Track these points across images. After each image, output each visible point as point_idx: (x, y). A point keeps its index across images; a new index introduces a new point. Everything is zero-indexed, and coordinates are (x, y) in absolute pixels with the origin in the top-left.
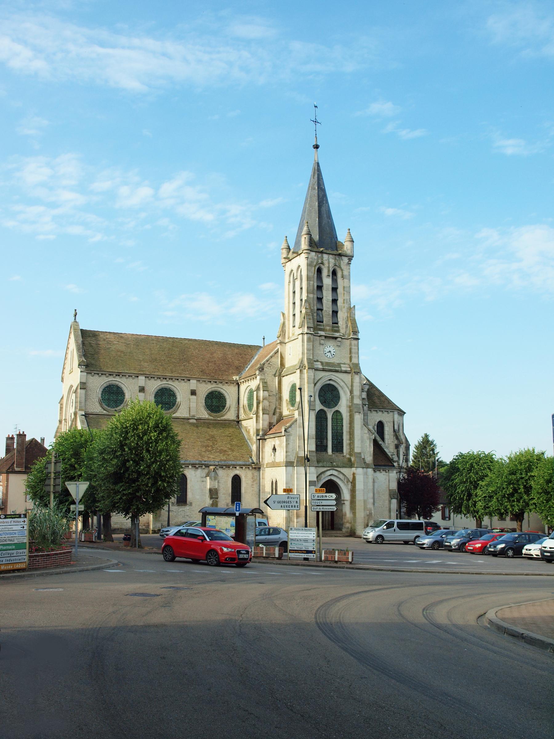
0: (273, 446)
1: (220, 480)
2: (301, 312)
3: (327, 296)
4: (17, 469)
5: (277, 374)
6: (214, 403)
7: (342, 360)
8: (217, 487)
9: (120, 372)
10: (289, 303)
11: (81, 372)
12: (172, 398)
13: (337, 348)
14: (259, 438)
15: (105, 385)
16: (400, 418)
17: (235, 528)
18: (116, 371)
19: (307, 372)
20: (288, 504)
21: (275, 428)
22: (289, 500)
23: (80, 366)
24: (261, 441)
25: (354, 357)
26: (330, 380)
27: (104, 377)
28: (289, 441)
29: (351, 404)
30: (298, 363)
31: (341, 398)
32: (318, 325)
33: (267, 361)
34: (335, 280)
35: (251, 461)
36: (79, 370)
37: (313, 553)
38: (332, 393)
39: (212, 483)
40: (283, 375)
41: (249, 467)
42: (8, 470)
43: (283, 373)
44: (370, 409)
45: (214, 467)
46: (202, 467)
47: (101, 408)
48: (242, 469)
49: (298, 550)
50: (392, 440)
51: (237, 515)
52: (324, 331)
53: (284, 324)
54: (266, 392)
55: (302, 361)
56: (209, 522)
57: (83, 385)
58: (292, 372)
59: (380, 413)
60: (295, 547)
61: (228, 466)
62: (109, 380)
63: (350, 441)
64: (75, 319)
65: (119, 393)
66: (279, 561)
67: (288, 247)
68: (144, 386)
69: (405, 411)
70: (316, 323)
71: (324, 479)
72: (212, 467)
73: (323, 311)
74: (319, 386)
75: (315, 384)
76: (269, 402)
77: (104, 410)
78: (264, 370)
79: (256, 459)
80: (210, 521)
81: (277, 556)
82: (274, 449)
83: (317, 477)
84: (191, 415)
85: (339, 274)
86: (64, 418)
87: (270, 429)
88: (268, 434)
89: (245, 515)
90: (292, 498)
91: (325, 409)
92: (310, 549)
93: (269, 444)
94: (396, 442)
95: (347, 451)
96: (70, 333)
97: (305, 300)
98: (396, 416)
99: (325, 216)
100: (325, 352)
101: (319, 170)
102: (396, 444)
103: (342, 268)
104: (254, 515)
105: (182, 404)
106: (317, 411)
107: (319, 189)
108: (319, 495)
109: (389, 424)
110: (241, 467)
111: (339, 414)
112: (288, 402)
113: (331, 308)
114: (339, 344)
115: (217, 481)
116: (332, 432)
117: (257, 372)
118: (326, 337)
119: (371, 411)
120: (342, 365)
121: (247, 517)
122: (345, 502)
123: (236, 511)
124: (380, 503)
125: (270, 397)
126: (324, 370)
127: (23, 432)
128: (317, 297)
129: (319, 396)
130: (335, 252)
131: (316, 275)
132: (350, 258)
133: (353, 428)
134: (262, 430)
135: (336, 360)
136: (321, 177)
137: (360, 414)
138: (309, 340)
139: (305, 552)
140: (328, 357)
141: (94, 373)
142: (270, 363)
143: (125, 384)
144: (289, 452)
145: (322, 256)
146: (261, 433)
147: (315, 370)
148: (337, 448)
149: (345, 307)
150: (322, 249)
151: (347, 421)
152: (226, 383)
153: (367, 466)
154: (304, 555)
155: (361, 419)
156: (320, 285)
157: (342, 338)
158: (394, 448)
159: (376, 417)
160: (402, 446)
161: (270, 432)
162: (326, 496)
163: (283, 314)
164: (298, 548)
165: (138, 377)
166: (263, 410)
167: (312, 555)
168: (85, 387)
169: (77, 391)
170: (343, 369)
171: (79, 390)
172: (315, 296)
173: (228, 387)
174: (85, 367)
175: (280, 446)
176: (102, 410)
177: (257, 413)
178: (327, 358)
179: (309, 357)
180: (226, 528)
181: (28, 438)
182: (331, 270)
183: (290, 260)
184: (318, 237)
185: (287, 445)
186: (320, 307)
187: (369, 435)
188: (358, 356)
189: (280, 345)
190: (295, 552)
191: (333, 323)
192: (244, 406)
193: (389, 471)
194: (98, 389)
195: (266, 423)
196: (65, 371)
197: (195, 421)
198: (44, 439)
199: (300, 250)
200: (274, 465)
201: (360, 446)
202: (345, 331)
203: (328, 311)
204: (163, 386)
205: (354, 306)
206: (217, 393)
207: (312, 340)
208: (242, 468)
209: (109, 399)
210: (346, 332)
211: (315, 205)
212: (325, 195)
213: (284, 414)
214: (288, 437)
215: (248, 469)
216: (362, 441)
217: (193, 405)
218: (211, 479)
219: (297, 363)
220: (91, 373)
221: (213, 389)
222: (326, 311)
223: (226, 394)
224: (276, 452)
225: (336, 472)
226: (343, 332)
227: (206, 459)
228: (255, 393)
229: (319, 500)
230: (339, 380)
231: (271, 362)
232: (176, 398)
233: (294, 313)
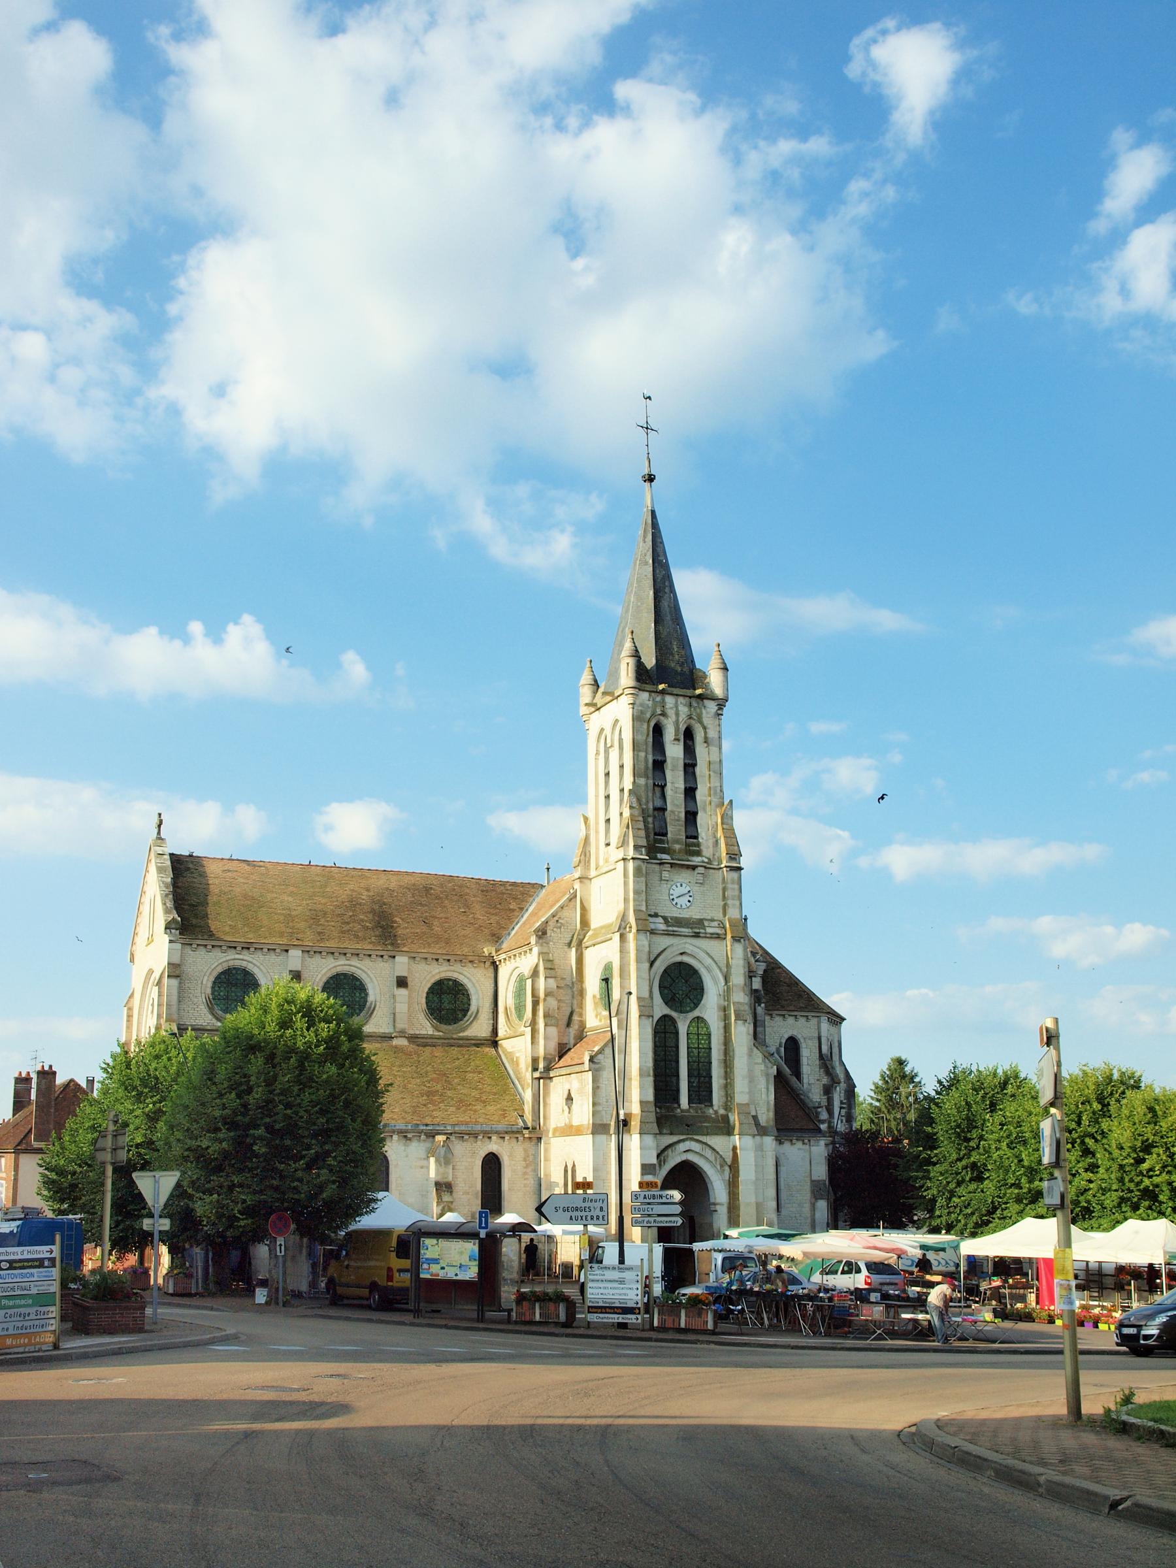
0: (566, 1093)
2: (621, 814)
3: (675, 781)
4: (36, 1145)
5: (574, 943)
6: (445, 1004)
8: (450, 1179)
9: (251, 941)
10: (597, 796)
11: (171, 941)
12: (358, 995)
13: (696, 888)
14: (537, 1075)
15: (220, 969)
16: (833, 1029)
17: (477, 1263)
18: (242, 940)
19: (637, 940)
20: (584, 1214)
21: (570, 1054)
22: (587, 1204)
23: (168, 930)
24: (541, 1081)
26: (681, 954)
27: (217, 953)
28: (598, 1081)
29: (726, 1003)
30: (617, 918)
31: (705, 990)
32: (656, 841)
33: (554, 916)
34: (689, 750)
35: (521, 1124)
36: (166, 938)
37: (635, 1313)
38: (686, 982)
39: (442, 1170)
40: (587, 944)
41: (517, 1136)
42: (17, 1146)
43: (587, 941)
44: (769, 1011)
45: (444, 1137)
47: (210, 1017)
48: (502, 1141)
49: (605, 1308)
50: (817, 1077)
51: (481, 1236)
52: (668, 854)
53: (587, 840)
54: (551, 981)
55: (624, 915)
56: (426, 1251)
57: (175, 970)
58: (602, 938)
59: (791, 1020)
60: (600, 1301)
61: (474, 1135)
62: (228, 958)
63: (727, 1080)
64: (159, 833)
65: (248, 984)
66: (569, 1331)
67: (593, 683)
68: (300, 969)
69: (843, 1015)
70: (652, 836)
71: (674, 1160)
72: (440, 1138)
73: (667, 813)
74: (660, 966)
75: (652, 964)
76: (559, 1001)
79: (533, 1120)
80: (427, 1249)
81: (563, 1317)
82: (569, 1098)
83: (658, 1156)
84: (397, 1030)
85: (699, 736)
86: (134, 1037)
87: (560, 1057)
88: (556, 1066)
89: (498, 1235)
90: (591, 1201)
91: (674, 1014)
92: (631, 1304)
93: (558, 1087)
94: (825, 1080)
95: (719, 1101)
96: (149, 861)
97: (630, 790)
98: (825, 1026)
99: (668, 618)
101: (655, 525)
102: (824, 1085)
103: (705, 725)
104: (518, 1235)
105: (377, 1007)
106: (656, 1019)
107: (656, 565)
108: (647, 1193)
109: (810, 1043)
111: (703, 1025)
112: (597, 1000)
114: (700, 878)
115: (451, 1167)
116: (688, 1062)
117: (533, 940)
118: (672, 865)
119: (771, 1015)
120: (706, 923)
121: (502, 1241)
122: (718, 1207)
123: (480, 1227)
124: (791, 1209)
125: (561, 991)
126: (667, 934)
127: (51, 1067)
128: (654, 784)
129: (659, 987)
130: (689, 692)
131: (650, 739)
132: (722, 703)
133: (731, 1054)
134: (544, 1058)
136: (659, 540)
137: (747, 1024)
138: (638, 872)
139: (620, 1311)
140: (679, 906)
141: (198, 945)
142: (560, 921)
143: (261, 967)
144: (599, 1104)
145: (663, 700)
146: (541, 1066)
147: (651, 933)
149: (713, 804)
150: (661, 687)
151: (718, 1039)
152: (470, 962)
153: (762, 1131)
154: (618, 1318)
155: (749, 1034)
156: (660, 758)
157: (705, 867)
158: (822, 1093)
159: (780, 1028)
160: (838, 1089)
161: (562, 1063)
162: (661, 1197)
163: (586, 819)
164: (606, 1303)
165: (287, 951)
166: (545, 1017)
167: (634, 1316)
168: (177, 973)
169: (163, 981)
170: (709, 930)
171: (166, 980)
172: (651, 782)
173: (473, 969)
174: (178, 931)
175: (581, 1091)
176: (214, 1021)
177: (533, 1024)
178: (676, 909)
179: (639, 908)
180: (461, 1264)
181: (60, 1080)
182: (682, 728)
183: (598, 709)
184: (654, 661)
185: (596, 1089)
187: (766, 1067)
188: (741, 904)
189: (581, 882)
190: (604, 1311)
191: (687, 837)
192: (506, 1008)
193: (809, 1141)
194: (206, 978)
195: (553, 1046)
196: (138, 940)
197: (403, 1042)
198: (94, 1080)
199: (617, 688)
200: (570, 1131)
201: (747, 1090)
202: (712, 852)
203: (676, 813)
205: (731, 801)
206: (451, 983)
207: (644, 872)
209: (227, 998)
210: (714, 855)
211: (648, 596)
212: (668, 577)
213: (587, 1026)
214: (598, 1073)
215: (515, 1140)
216: (751, 1079)
217: (402, 1008)
218: (437, 1161)
219: (614, 919)
220: (191, 944)
222: (672, 812)
223: (469, 986)
224: (574, 1106)
226: (708, 856)
227: (428, 1120)
228: (529, 982)
229: (649, 1204)
231: (562, 917)
232: (367, 995)
233: (607, 818)
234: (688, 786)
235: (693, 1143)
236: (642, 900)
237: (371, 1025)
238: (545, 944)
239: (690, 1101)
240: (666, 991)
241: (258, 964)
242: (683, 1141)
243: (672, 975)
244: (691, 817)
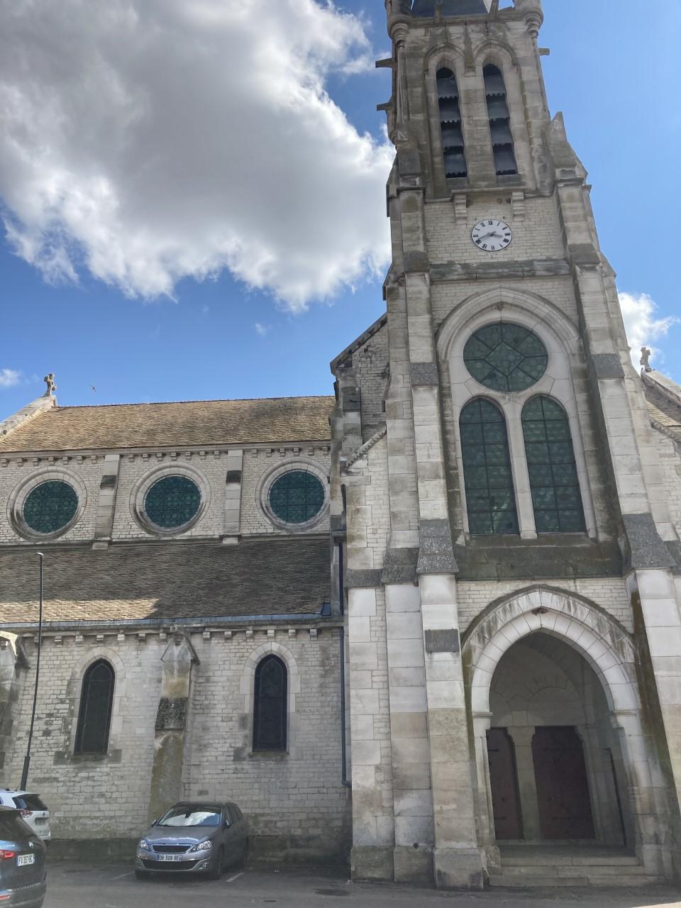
1: (218, 673)
3: (475, 118)
6: (293, 500)
46: (158, 634)
48: (279, 637)
77: (21, 535)
78: (351, 366)
110: (281, 627)
113: (489, 138)
176: (17, 536)
178: (484, 253)
186: (451, 142)
191: (499, 173)
203: (478, 148)
204: (166, 472)
208: (287, 631)
210: (542, 182)
221: (289, 467)
231: (372, 344)
232: (199, 497)
234: (495, 117)
236: (419, 238)
237: (198, 529)
238: (349, 378)
240: (479, 365)
242: (526, 591)
244: (504, 150)
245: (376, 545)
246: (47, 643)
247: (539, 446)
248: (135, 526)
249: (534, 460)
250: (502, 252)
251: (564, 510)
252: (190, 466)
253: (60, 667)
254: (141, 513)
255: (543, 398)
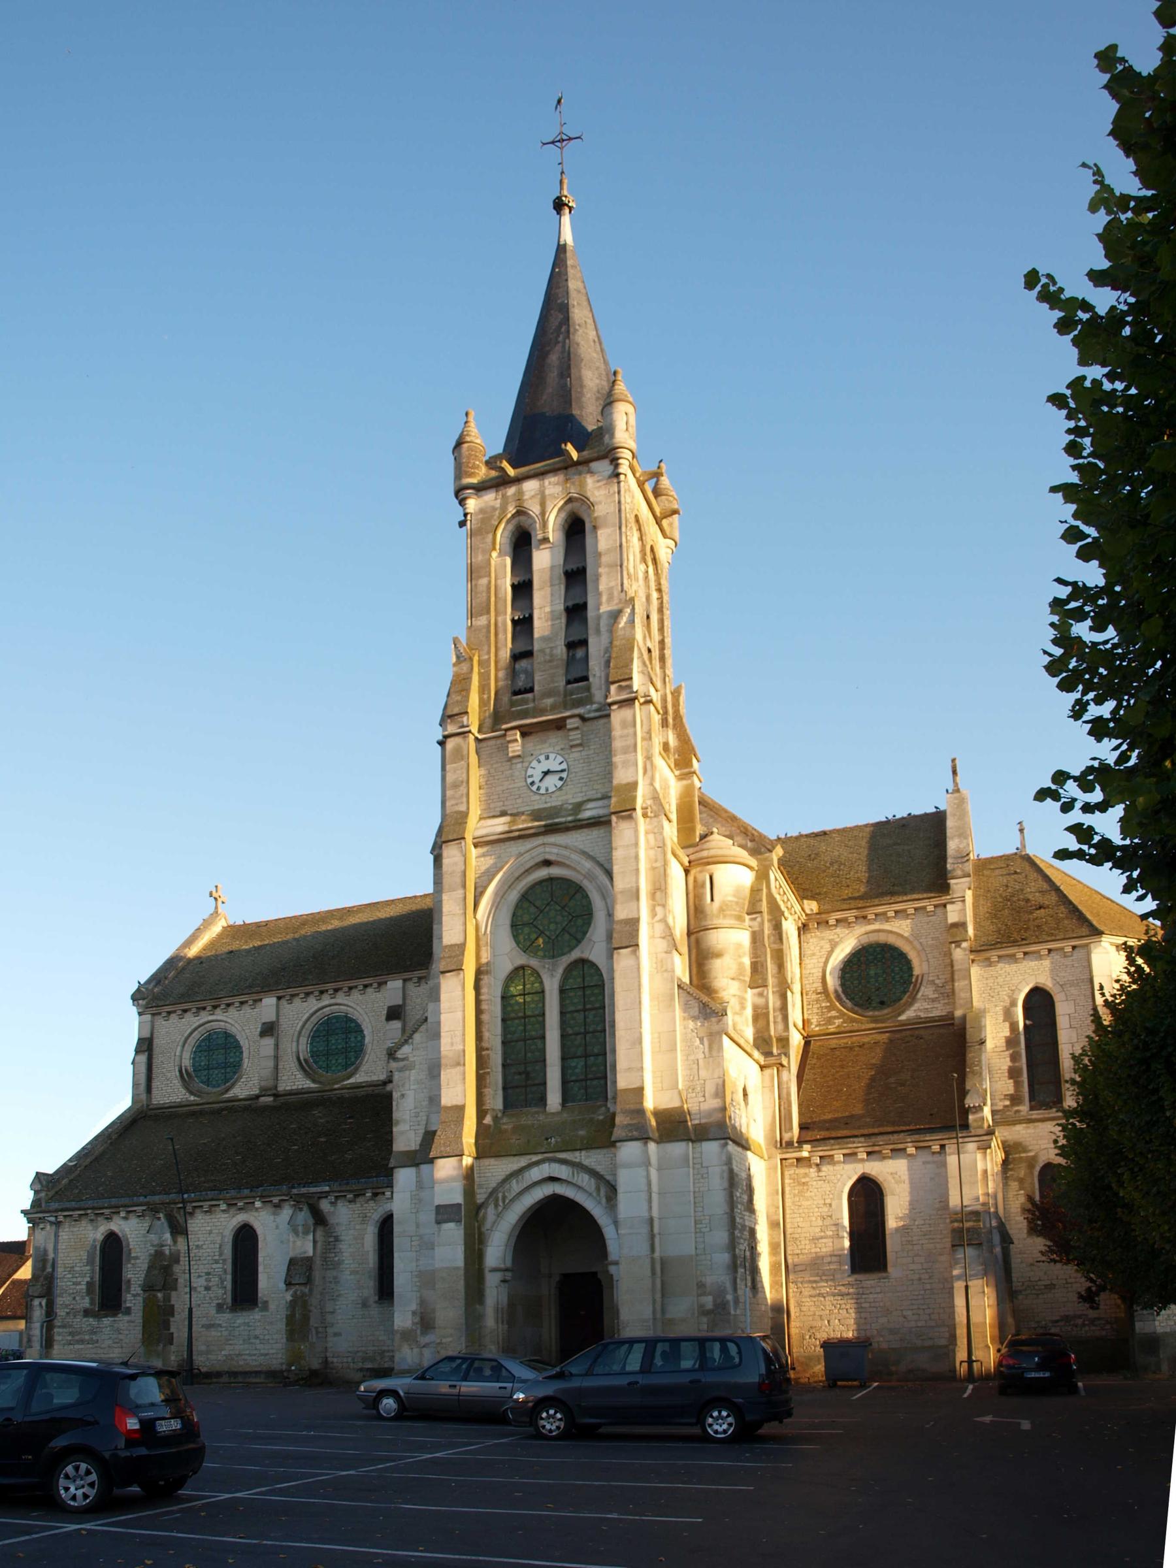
7: (596, 787)
25: (620, 766)
38: (563, 908)
91: (534, 963)
100: (529, 780)
111: (592, 971)
135: (572, 796)
140: (542, 791)
148: (586, 1088)
178: (537, 797)
225: (564, 1167)
230: (574, 856)
235: (555, 1166)
239: (566, 1097)
241: (300, 1024)
243: (538, 903)
245: (417, 1127)
246: (198, 1211)
247: (575, 1014)
248: (299, 1075)
249: (539, 1042)
250: (558, 793)
251: (591, 1079)
252: (350, 1004)
253: (210, 1232)
254: (306, 1060)
255: (583, 962)
